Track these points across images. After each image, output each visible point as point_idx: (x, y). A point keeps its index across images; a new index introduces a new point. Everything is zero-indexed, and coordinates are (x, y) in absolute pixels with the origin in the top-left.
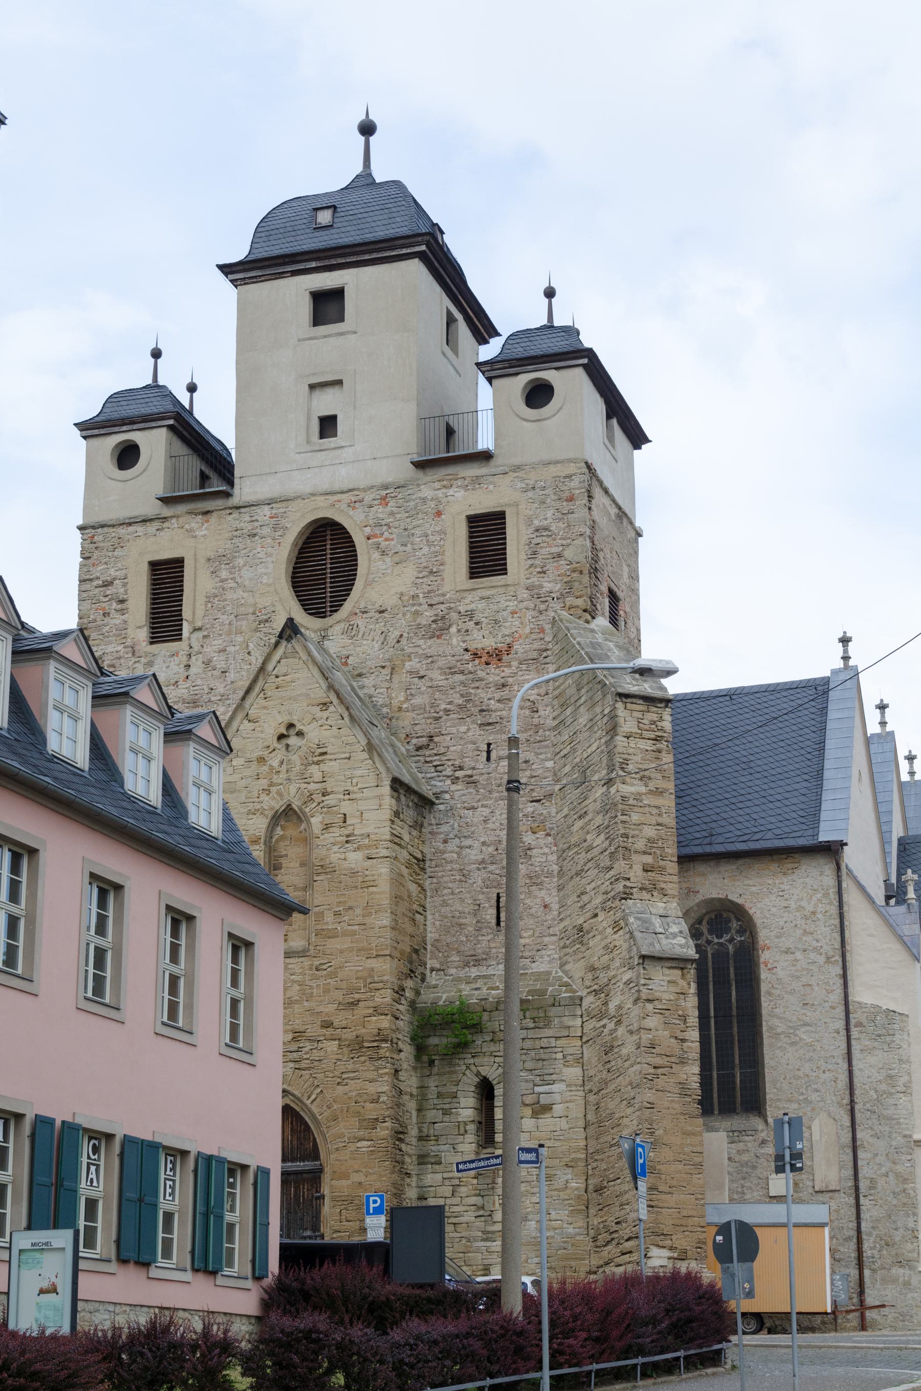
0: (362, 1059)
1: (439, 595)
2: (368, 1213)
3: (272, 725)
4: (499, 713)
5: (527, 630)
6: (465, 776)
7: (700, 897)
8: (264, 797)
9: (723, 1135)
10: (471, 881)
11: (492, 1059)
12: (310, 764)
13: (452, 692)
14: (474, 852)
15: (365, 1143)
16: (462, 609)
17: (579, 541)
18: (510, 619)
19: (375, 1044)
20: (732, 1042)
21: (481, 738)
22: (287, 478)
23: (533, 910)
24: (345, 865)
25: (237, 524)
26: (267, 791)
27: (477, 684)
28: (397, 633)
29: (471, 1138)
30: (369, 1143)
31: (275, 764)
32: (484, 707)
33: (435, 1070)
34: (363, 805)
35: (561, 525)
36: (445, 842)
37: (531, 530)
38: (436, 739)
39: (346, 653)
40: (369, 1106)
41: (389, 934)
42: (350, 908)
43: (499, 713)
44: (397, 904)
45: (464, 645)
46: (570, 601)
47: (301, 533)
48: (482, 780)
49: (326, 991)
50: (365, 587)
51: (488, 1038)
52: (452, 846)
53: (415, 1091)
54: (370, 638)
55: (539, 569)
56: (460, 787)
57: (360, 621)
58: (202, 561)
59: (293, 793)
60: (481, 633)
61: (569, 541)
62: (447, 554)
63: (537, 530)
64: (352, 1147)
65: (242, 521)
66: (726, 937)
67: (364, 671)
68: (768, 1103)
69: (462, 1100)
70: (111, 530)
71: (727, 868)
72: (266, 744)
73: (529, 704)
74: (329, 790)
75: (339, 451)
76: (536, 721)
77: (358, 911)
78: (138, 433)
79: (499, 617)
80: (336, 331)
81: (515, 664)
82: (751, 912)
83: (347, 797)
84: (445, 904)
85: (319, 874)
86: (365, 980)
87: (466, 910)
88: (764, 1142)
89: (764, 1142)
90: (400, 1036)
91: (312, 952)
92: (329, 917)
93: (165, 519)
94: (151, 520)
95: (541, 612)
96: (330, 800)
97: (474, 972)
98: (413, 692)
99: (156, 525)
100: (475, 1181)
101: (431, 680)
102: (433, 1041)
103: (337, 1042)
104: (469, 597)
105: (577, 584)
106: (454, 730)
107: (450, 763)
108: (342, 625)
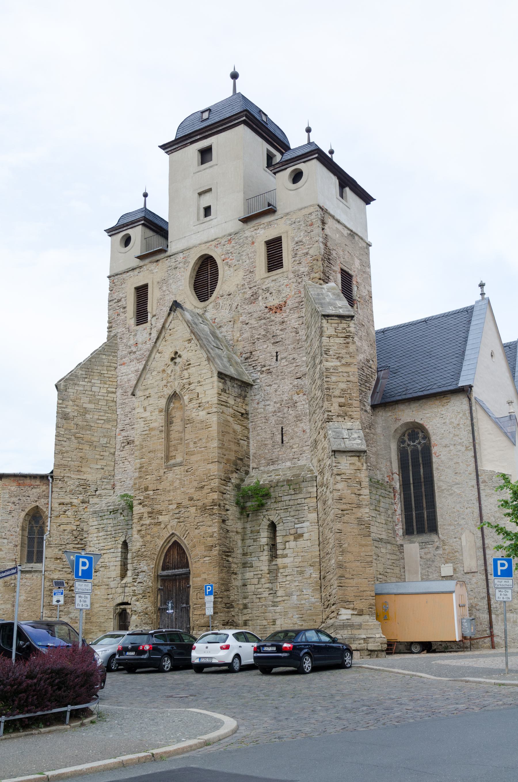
0: (206, 515)
1: (254, 282)
2: (206, 595)
3: (168, 353)
4: (281, 336)
5: (293, 293)
6: (267, 370)
7: (401, 422)
8: (165, 389)
9: (417, 545)
10: (269, 422)
11: (275, 511)
12: (183, 370)
13: (260, 329)
14: (271, 407)
15: (207, 558)
16: (264, 287)
17: (316, 245)
18: (285, 289)
19: (212, 507)
20: (422, 496)
21: (273, 349)
22: (189, 238)
23: (298, 434)
24: (198, 418)
25: (169, 264)
26: (166, 386)
27: (271, 323)
28: (236, 304)
29: (266, 553)
30: (209, 558)
31: (169, 372)
32: (274, 335)
33: (250, 519)
34: (206, 387)
35: (308, 238)
36: (258, 404)
37: (294, 243)
38: (253, 353)
39: (214, 317)
40: (209, 539)
41: (216, 450)
42: (200, 439)
43: (281, 336)
44: (223, 436)
45: (265, 305)
46: (313, 275)
47: (196, 264)
48: (274, 370)
49: (191, 482)
50: (222, 284)
51: (273, 501)
52: (261, 405)
53: (240, 530)
54: (224, 308)
55: (298, 262)
56: (264, 376)
57: (220, 301)
58: (155, 283)
59: (176, 386)
60: (272, 298)
61: (311, 246)
62: (257, 262)
63: (297, 243)
64: (202, 560)
65: (171, 262)
66: (417, 442)
67: (222, 325)
68: (439, 527)
69: (262, 534)
70: (120, 276)
71: (414, 406)
72: (166, 363)
73: (295, 330)
74: (191, 382)
75: (211, 222)
76: (298, 338)
77: (204, 441)
78: (130, 230)
79: (280, 289)
80: (208, 166)
81: (288, 311)
82: (427, 427)
83: (199, 384)
84: (258, 435)
85: (187, 424)
86: (206, 474)
87: (268, 437)
88: (438, 548)
89: (438, 548)
90: (227, 502)
91: (184, 463)
92: (192, 445)
93: (141, 267)
94: (135, 268)
95: (299, 283)
96: (192, 387)
97: (272, 468)
98: (243, 331)
99: (138, 270)
100: (268, 575)
101: (251, 324)
102: (249, 504)
103: (195, 507)
104: (267, 281)
105: (315, 266)
106: (261, 348)
107: (259, 364)
108: (213, 304)
